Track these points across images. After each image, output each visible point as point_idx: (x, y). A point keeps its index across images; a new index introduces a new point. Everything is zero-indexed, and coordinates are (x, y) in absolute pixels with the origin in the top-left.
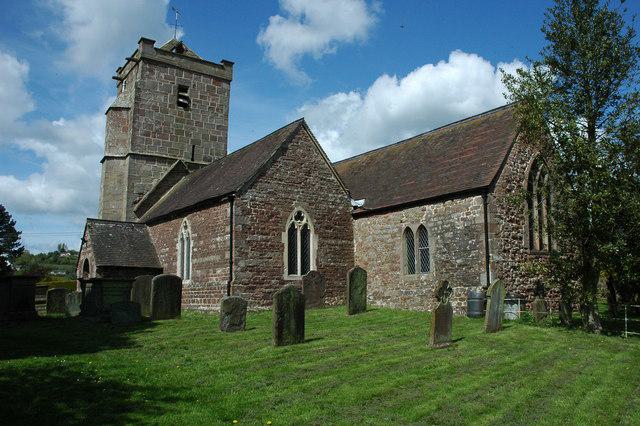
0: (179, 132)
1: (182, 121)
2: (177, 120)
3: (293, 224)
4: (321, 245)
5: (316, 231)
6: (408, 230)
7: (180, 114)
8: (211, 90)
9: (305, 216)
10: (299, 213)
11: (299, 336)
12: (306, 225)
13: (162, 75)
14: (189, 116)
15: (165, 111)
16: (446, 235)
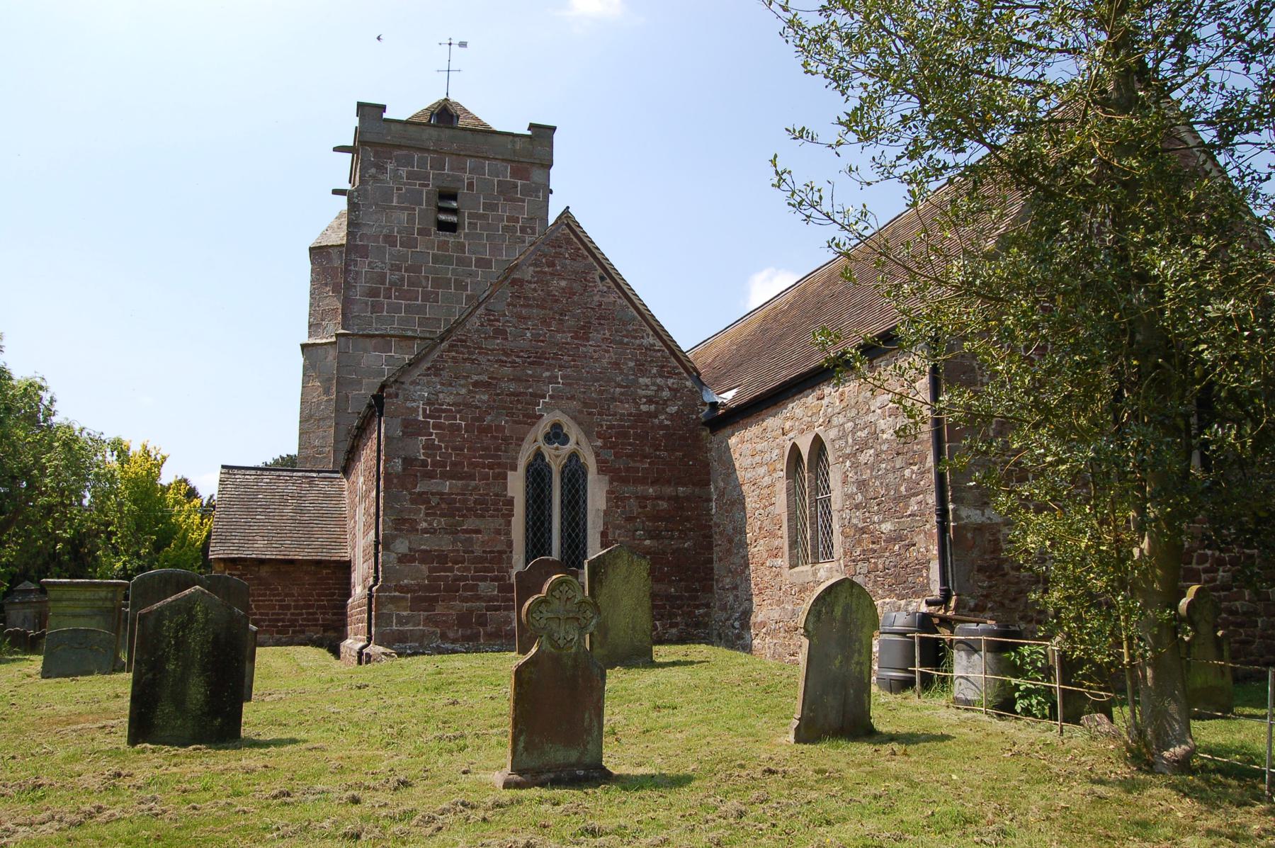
0: (440, 283)
1: (448, 260)
2: (436, 259)
3: (539, 455)
4: (615, 499)
5: (603, 468)
6: (795, 449)
7: (443, 245)
8: (506, 190)
9: (573, 432)
10: (557, 426)
11: (219, 723)
12: (574, 456)
13: (403, 172)
14: (461, 247)
15: (410, 243)
16: (863, 458)
